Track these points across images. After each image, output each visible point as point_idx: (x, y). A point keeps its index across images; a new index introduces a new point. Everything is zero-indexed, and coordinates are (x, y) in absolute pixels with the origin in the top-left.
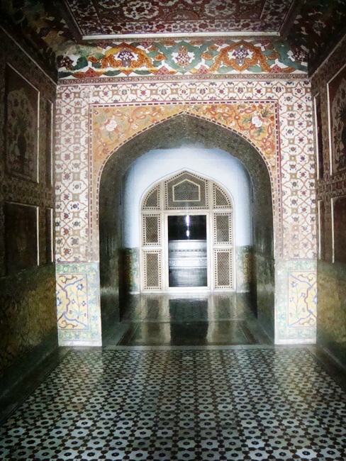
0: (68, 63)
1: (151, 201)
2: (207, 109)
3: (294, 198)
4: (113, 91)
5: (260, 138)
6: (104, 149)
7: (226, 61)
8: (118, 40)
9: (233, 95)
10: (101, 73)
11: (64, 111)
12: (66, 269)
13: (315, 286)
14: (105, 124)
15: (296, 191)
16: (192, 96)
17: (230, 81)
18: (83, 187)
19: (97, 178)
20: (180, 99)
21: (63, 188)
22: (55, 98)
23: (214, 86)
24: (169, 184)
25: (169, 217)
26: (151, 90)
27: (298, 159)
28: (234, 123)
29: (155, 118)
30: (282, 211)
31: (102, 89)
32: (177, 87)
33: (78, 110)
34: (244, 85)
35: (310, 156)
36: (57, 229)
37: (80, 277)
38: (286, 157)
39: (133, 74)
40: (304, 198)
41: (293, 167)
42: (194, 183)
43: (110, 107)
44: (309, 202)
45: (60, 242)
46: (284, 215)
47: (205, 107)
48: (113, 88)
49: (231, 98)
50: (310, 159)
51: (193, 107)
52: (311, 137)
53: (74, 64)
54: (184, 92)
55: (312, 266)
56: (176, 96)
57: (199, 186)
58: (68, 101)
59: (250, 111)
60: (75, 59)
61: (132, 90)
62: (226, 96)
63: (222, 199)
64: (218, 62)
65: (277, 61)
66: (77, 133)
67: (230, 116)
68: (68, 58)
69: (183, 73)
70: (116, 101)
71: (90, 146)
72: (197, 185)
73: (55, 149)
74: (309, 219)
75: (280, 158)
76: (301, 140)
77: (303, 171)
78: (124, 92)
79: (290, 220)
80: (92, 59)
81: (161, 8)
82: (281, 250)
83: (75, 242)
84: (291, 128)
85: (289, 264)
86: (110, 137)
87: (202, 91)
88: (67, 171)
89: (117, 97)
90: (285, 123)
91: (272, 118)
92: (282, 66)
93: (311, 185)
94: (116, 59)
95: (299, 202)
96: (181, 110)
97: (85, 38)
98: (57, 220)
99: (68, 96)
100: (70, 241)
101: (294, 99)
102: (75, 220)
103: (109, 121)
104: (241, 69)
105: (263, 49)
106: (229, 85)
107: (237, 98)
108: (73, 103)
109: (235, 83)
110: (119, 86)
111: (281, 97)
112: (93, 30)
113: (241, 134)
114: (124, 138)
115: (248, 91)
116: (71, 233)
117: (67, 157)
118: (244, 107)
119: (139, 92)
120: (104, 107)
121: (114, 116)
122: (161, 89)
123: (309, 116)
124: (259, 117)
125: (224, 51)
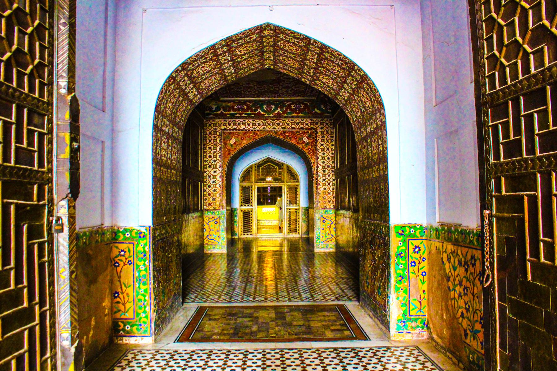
0: (211, 109)
1: (246, 176)
3: (324, 178)
5: (307, 148)
7: (291, 109)
8: (237, 100)
9: (294, 126)
11: (208, 133)
12: (209, 213)
13: (334, 222)
15: (325, 175)
18: (218, 172)
19: (225, 167)
21: (208, 173)
22: (204, 126)
24: (258, 166)
25: (258, 188)
27: (326, 159)
28: (294, 141)
30: (318, 185)
31: (228, 121)
33: (215, 133)
35: (332, 157)
36: (205, 193)
37: (216, 218)
38: (320, 158)
39: (243, 115)
40: (329, 178)
41: (323, 162)
44: (331, 180)
45: (206, 199)
46: (319, 187)
47: (280, 132)
49: (293, 128)
50: (332, 159)
52: (333, 147)
53: (214, 109)
54: (269, 124)
55: (333, 212)
56: (265, 127)
58: (210, 128)
60: (214, 107)
62: (291, 126)
63: (293, 176)
64: (286, 110)
65: (316, 109)
66: (215, 144)
67: (292, 137)
68: (211, 106)
69: (269, 115)
70: (235, 129)
71: (222, 151)
73: (205, 152)
74: (331, 189)
75: (317, 158)
76: (328, 149)
77: (328, 164)
78: (239, 124)
79: (322, 189)
80: (223, 108)
81: (259, 91)
82: (317, 204)
83: (214, 199)
84: (323, 143)
85: (322, 211)
87: (279, 124)
88: (210, 164)
89: (236, 127)
90: (320, 140)
91: (313, 138)
92: (318, 111)
93: (333, 171)
94: (235, 107)
95: (327, 180)
97: (221, 99)
98: (205, 188)
99: (210, 125)
100: (211, 199)
101: (325, 128)
102: (214, 188)
104: (298, 113)
105: (308, 104)
108: (212, 129)
111: (318, 128)
112: (224, 97)
114: (239, 147)
116: (212, 195)
117: (210, 157)
118: (299, 132)
119: (246, 124)
123: (332, 137)
125: (289, 106)
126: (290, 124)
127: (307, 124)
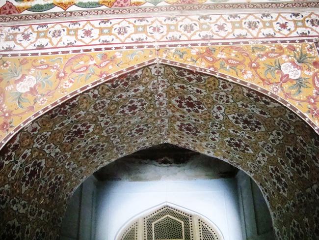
2: (198, 53)
4: (39, 33)
5: (303, 96)
6: (5, 123)
9: (243, 32)
10: (24, 9)
14: (17, 82)
16: (171, 35)
17: (234, 12)
20: (150, 39)
23: (208, 20)
26: (101, 29)
29: (104, 70)
32: (144, 23)
34: (256, 18)
42: (177, 220)
43: (30, 56)
47: (194, 52)
48: (40, 29)
51: (173, 51)
56: (143, 36)
57: (183, 223)
59: (273, 55)
61: (69, 30)
67: (241, 63)
70: (41, 47)
72: (179, 221)
86: (19, 102)
87: (189, 28)
89: (43, 41)
96: (151, 57)
103: (23, 77)
106: (232, 19)
107: (249, 36)
109: (242, 16)
110: (49, 26)
113: (267, 92)
114: (44, 104)
115: (265, 27)
119: (81, 33)
120: (19, 57)
121: (33, 70)
122: (117, 26)
124: (293, 63)
126: (228, 27)
127: (284, 26)
